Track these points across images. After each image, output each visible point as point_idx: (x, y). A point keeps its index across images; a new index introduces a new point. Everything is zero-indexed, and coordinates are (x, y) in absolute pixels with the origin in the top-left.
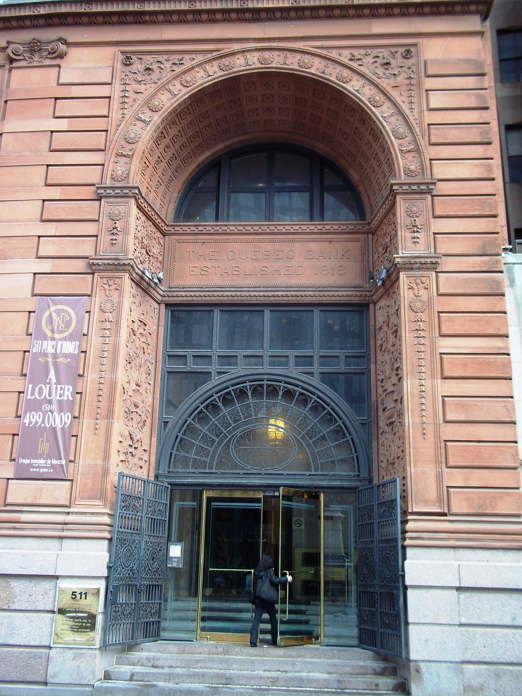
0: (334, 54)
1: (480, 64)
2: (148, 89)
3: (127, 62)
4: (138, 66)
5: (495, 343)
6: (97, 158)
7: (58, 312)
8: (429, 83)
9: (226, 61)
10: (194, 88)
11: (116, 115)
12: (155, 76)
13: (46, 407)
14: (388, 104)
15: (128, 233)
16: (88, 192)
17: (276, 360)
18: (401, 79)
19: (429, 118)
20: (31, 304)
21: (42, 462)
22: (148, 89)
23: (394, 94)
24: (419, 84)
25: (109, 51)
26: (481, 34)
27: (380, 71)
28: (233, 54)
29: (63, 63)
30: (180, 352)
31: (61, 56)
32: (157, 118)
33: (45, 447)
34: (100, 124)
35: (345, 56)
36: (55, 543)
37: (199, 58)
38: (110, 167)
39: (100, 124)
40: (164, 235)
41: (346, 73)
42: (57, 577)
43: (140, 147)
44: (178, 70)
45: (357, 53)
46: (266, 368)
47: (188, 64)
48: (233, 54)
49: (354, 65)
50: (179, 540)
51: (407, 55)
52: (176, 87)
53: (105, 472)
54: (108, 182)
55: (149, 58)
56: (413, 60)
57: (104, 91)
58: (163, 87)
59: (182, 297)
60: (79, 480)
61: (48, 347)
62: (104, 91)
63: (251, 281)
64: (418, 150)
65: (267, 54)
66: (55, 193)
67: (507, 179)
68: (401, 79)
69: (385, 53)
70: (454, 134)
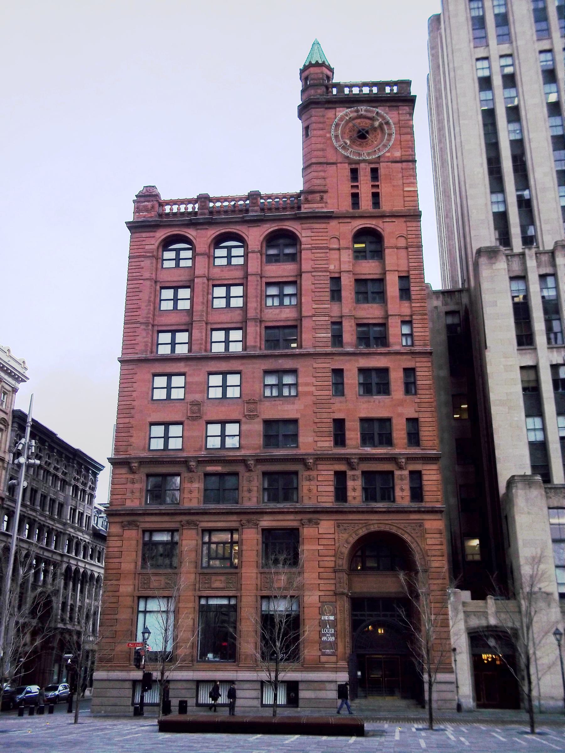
0: (398, 526)
1: (440, 530)
2: (345, 536)
3: (338, 526)
4: (341, 528)
5: (445, 616)
6: (333, 559)
7: (327, 607)
8: (427, 536)
9: (368, 527)
10: (359, 536)
11: (337, 545)
12: (348, 531)
13: (328, 635)
14: (415, 543)
15: (344, 583)
16: (331, 570)
17: (385, 616)
18: (418, 534)
19: (427, 547)
20: (319, 605)
21: (328, 651)
22: (345, 536)
23: (417, 539)
24: (424, 536)
25: (332, 522)
26: (441, 520)
27: (413, 532)
28: (370, 525)
29: (319, 526)
30: (355, 613)
31: (319, 524)
32: (349, 546)
33: (328, 646)
34: (333, 547)
35: (402, 526)
36: (335, 673)
37: (360, 526)
38: (337, 562)
39: (333, 547)
40: (348, 575)
41: (403, 532)
42: (336, 682)
43: (345, 556)
44: (355, 529)
45: (406, 525)
46: (382, 618)
47: (357, 528)
48: (370, 525)
49: (405, 529)
50: (359, 670)
51: (420, 526)
52: (354, 535)
53: (345, 653)
54: (337, 568)
55: (345, 525)
56: (422, 528)
57: (332, 536)
58: (351, 536)
59: (356, 596)
60: (338, 655)
61: (326, 618)
62: (332, 536)
63: (375, 590)
64: (424, 558)
65: (380, 525)
66: (322, 570)
67: (460, 510)
68: (418, 534)
69: (413, 525)
70: (434, 553)
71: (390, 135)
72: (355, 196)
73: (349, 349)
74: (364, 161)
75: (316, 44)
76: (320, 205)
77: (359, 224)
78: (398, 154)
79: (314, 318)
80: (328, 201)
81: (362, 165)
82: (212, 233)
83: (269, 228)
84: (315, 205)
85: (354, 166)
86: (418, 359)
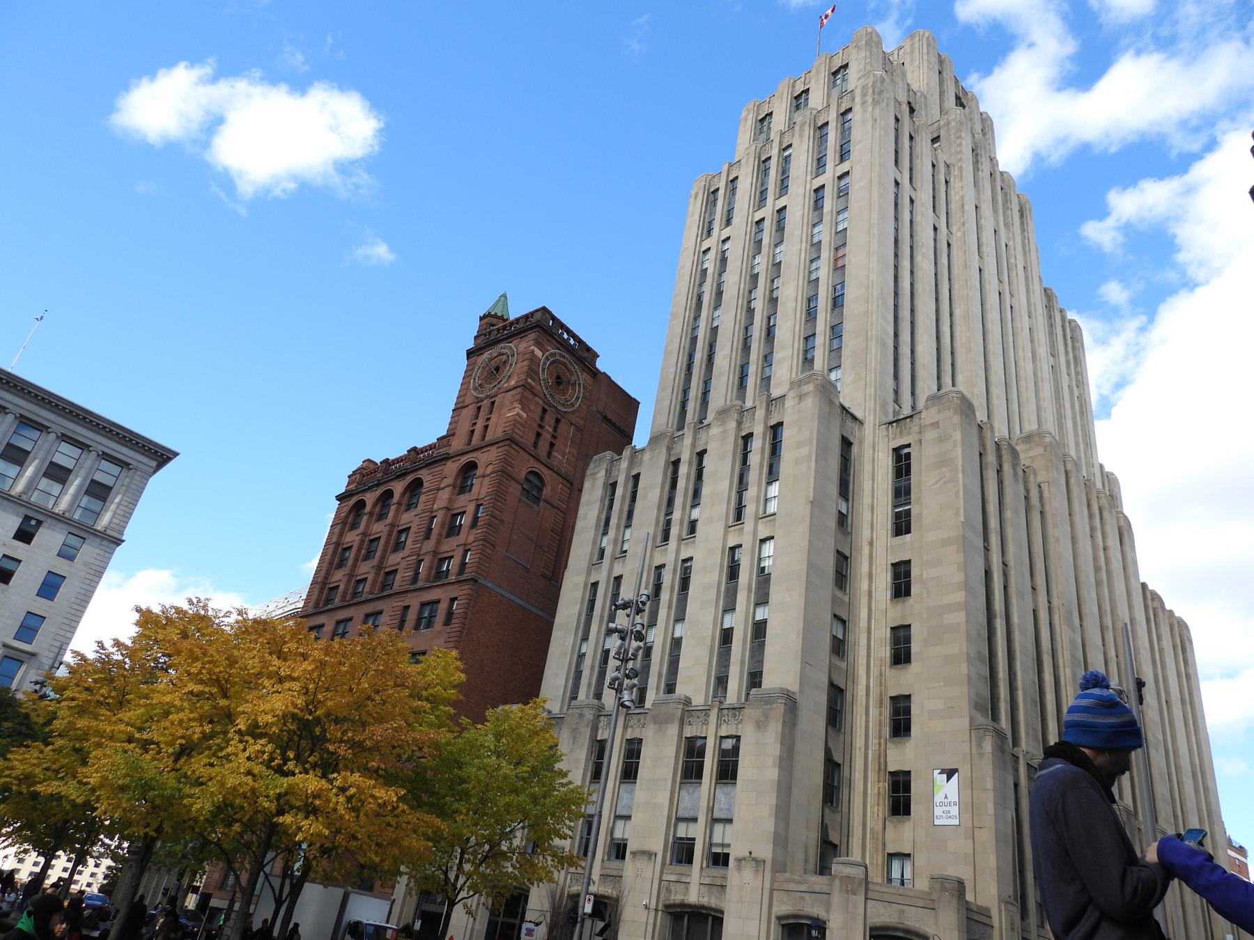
71: (511, 365)
72: (473, 432)
73: (420, 584)
74: (487, 397)
75: (504, 296)
76: (445, 449)
77: (464, 459)
78: (513, 383)
79: (408, 559)
80: (453, 443)
81: (485, 402)
82: (378, 492)
83: (410, 478)
84: (441, 450)
85: (480, 404)
86: (462, 588)
